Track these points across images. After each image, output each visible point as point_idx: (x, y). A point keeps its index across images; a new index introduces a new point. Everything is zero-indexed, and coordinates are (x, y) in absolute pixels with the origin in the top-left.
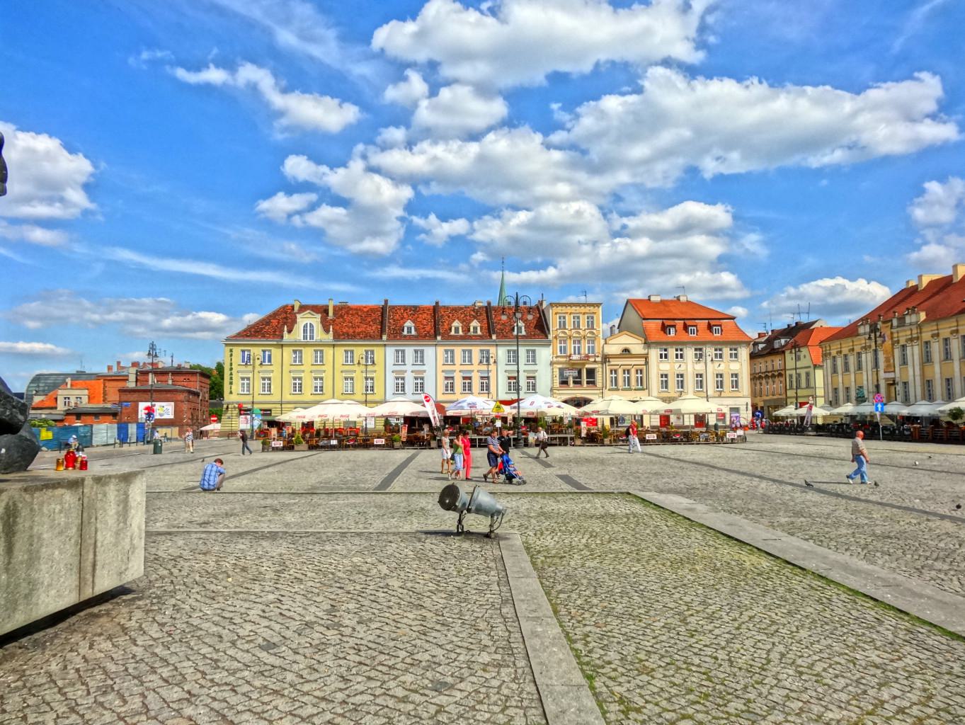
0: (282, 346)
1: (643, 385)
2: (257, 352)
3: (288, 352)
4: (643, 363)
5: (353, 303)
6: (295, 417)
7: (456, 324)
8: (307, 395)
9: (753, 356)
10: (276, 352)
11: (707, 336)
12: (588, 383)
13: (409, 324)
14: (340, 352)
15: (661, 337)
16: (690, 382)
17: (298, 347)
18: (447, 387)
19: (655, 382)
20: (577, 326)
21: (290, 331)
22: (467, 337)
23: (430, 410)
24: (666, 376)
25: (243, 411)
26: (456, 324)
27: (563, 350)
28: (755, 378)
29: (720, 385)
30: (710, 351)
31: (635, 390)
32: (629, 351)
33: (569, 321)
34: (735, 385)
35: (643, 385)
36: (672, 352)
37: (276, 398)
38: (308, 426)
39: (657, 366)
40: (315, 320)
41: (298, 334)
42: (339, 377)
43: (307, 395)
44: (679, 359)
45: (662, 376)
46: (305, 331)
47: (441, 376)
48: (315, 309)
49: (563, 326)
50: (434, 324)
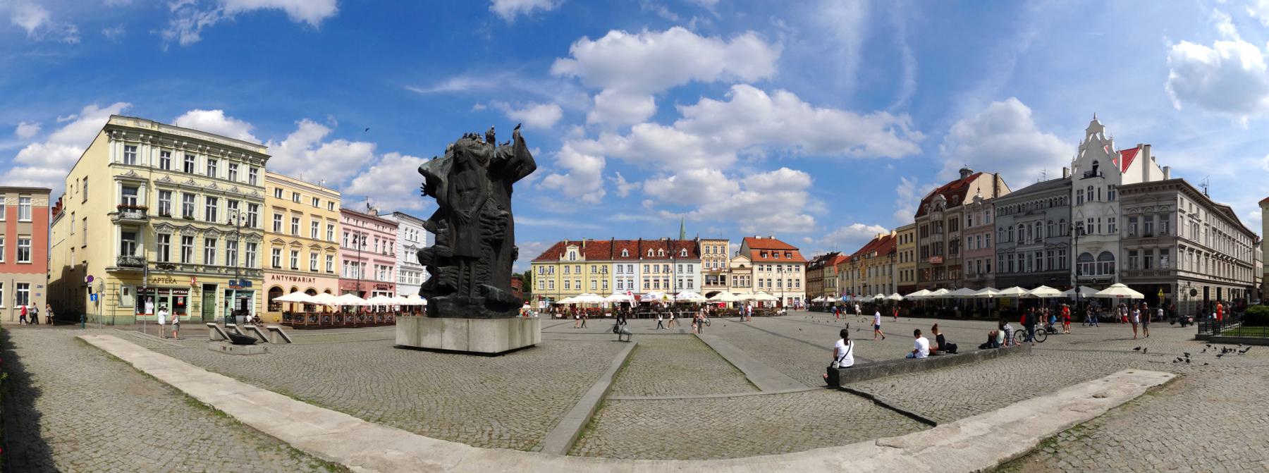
1: (750, 285)
2: (547, 267)
3: (562, 266)
5: (596, 239)
6: (566, 301)
8: (572, 290)
9: (807, 270)
10: (556, 267)
11: (783, 258)
14: (589, 266)
15: (760, 259)
16: (774, 283)
17: (567, 264)
19: (756, 282)
20: (715, 252)
22: (657, 258)
23: (631, 299)
25: (541, 299)
27: (708, 265)
28: (808, 281)
29: (790, 285)
30: (785, 267)
33: (711, 249)
34: (798, 285)
35: (750, 285)
36: (765, 267)
38: (573, 306)
40: (576, 250)
41: (567, 257)
42: (589, 280)
43: (572, 290)
48: (576, 243)
49: (708, 251)
50: (638, 251)
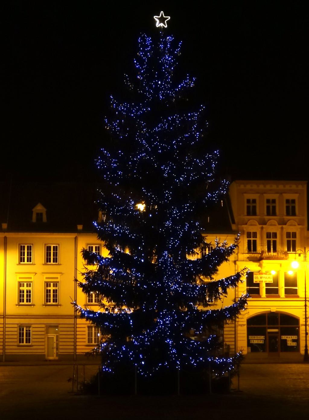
13: (39, 208)
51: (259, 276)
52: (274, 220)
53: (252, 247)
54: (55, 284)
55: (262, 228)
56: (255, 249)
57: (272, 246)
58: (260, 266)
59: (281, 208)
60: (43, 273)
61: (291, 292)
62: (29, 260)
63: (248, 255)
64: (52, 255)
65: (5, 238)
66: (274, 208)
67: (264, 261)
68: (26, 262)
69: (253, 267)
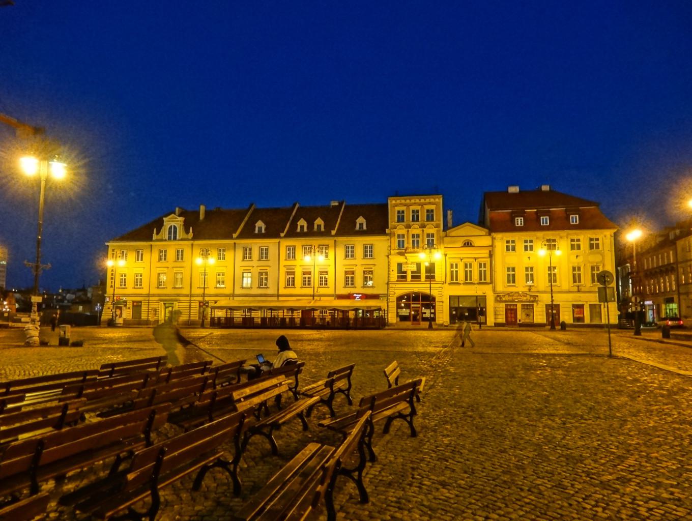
0: (151, 245)
4: (487, 255)
7: (302, 222)
12: (427, 277)
18: (288, 281)
21: (158, 233)
22: (311, 233)
24: (513, 269)
26: (302, 222)
31: (480, 283)
32: (471, 244)
37: (145, 291)
39: (503, 260)
44: (529, 252)
45: (509, 269)
46: (170, 233)
47: (283, 270)
51: (406, 266)
52: (416, 225)
53: (401, 245)
54: (267, 274)
55: (408, 231)
56: (403, 247)
57: (416, 244)
58: (406, 258)
59: (423, 216)
60: (258, 266)
61: (430, 277)
62: (250, 258)
63: (398, 251)
64: (264, 254)
65: (235, 243)
66: (418, 216)
67: (406, 255)
68: (248, 259)
69: (401, 259)
